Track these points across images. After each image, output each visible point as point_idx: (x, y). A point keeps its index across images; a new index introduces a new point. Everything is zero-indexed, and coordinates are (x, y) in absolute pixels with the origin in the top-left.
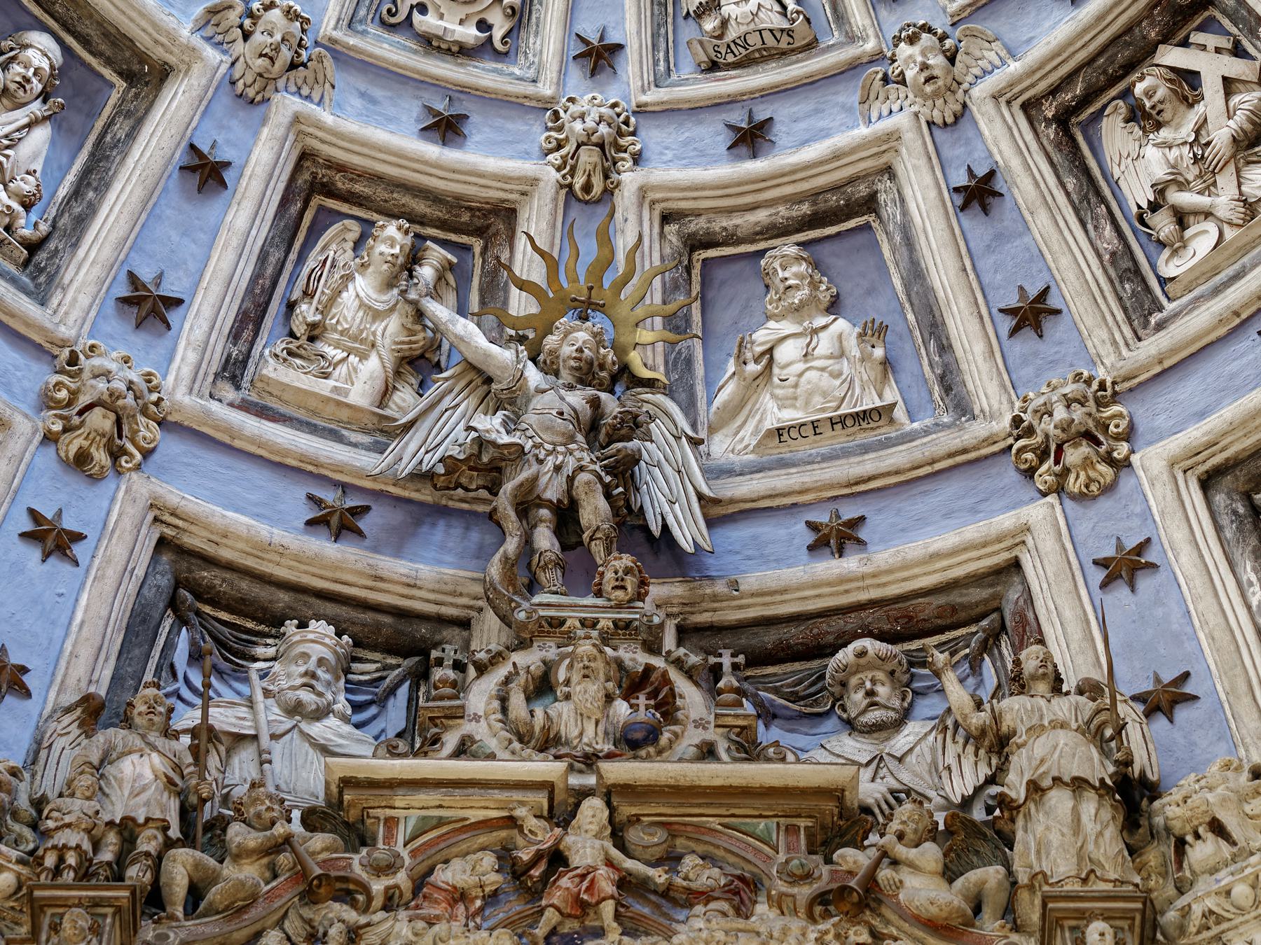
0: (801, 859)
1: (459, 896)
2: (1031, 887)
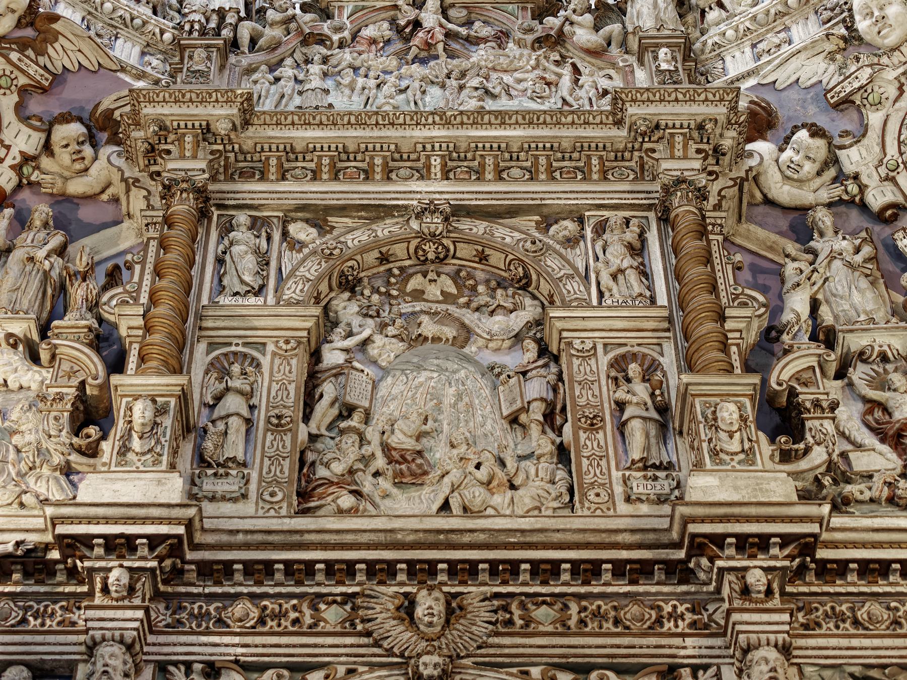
0: (529, 22)
1: (373, 41)
2: (634, 33)
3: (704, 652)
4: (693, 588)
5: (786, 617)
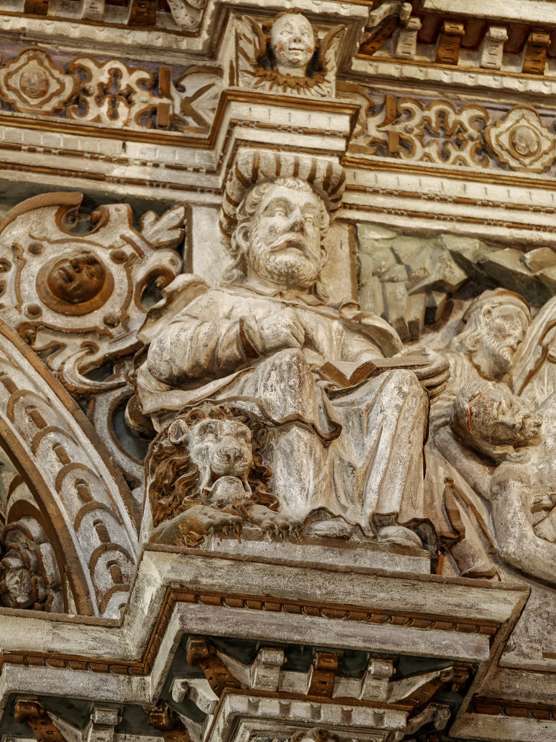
3: (163, 175)
4: (158, 39)
5: (341, 123)
